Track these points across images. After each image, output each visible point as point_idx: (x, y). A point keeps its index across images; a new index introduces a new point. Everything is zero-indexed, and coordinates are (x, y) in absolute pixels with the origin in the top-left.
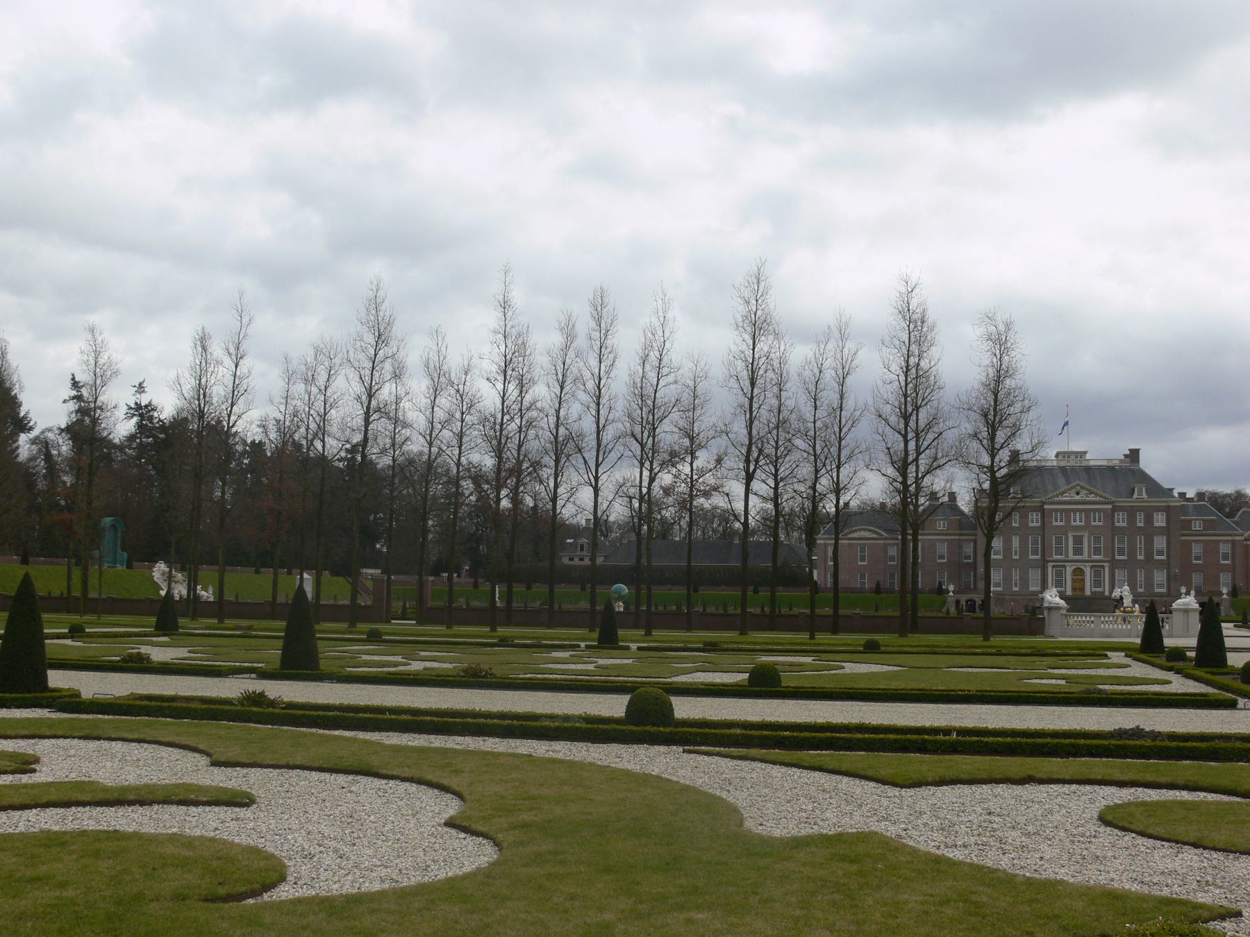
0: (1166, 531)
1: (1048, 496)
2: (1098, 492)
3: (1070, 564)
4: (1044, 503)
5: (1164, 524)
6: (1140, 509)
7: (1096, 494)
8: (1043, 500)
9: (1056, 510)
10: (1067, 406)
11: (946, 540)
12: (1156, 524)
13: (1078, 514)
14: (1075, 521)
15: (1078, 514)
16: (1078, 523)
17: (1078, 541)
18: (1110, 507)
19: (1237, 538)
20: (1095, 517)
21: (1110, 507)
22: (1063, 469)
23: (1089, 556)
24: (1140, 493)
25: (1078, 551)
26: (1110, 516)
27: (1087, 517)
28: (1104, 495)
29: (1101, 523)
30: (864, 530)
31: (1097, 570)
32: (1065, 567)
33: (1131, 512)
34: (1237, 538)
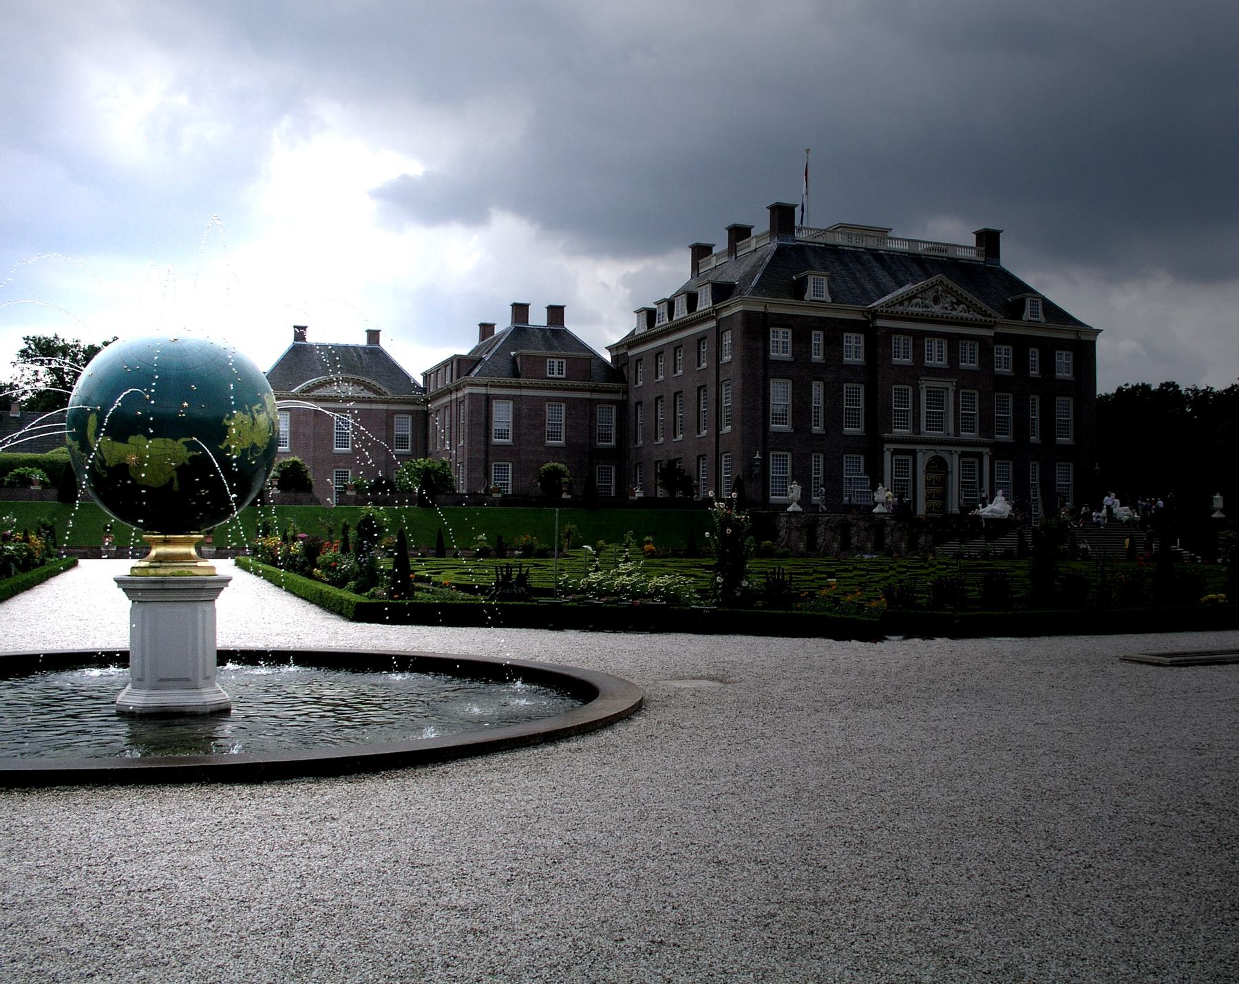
3: (923, 447)
4: (875, 315)
7: (970, 306)
10: (808, 151)
11: (564, 400)
17: (936, 398)
23: (957, 433)
25: (936, 421)
29: (975, 366)
31: (970, 458)
32: (913, 453)
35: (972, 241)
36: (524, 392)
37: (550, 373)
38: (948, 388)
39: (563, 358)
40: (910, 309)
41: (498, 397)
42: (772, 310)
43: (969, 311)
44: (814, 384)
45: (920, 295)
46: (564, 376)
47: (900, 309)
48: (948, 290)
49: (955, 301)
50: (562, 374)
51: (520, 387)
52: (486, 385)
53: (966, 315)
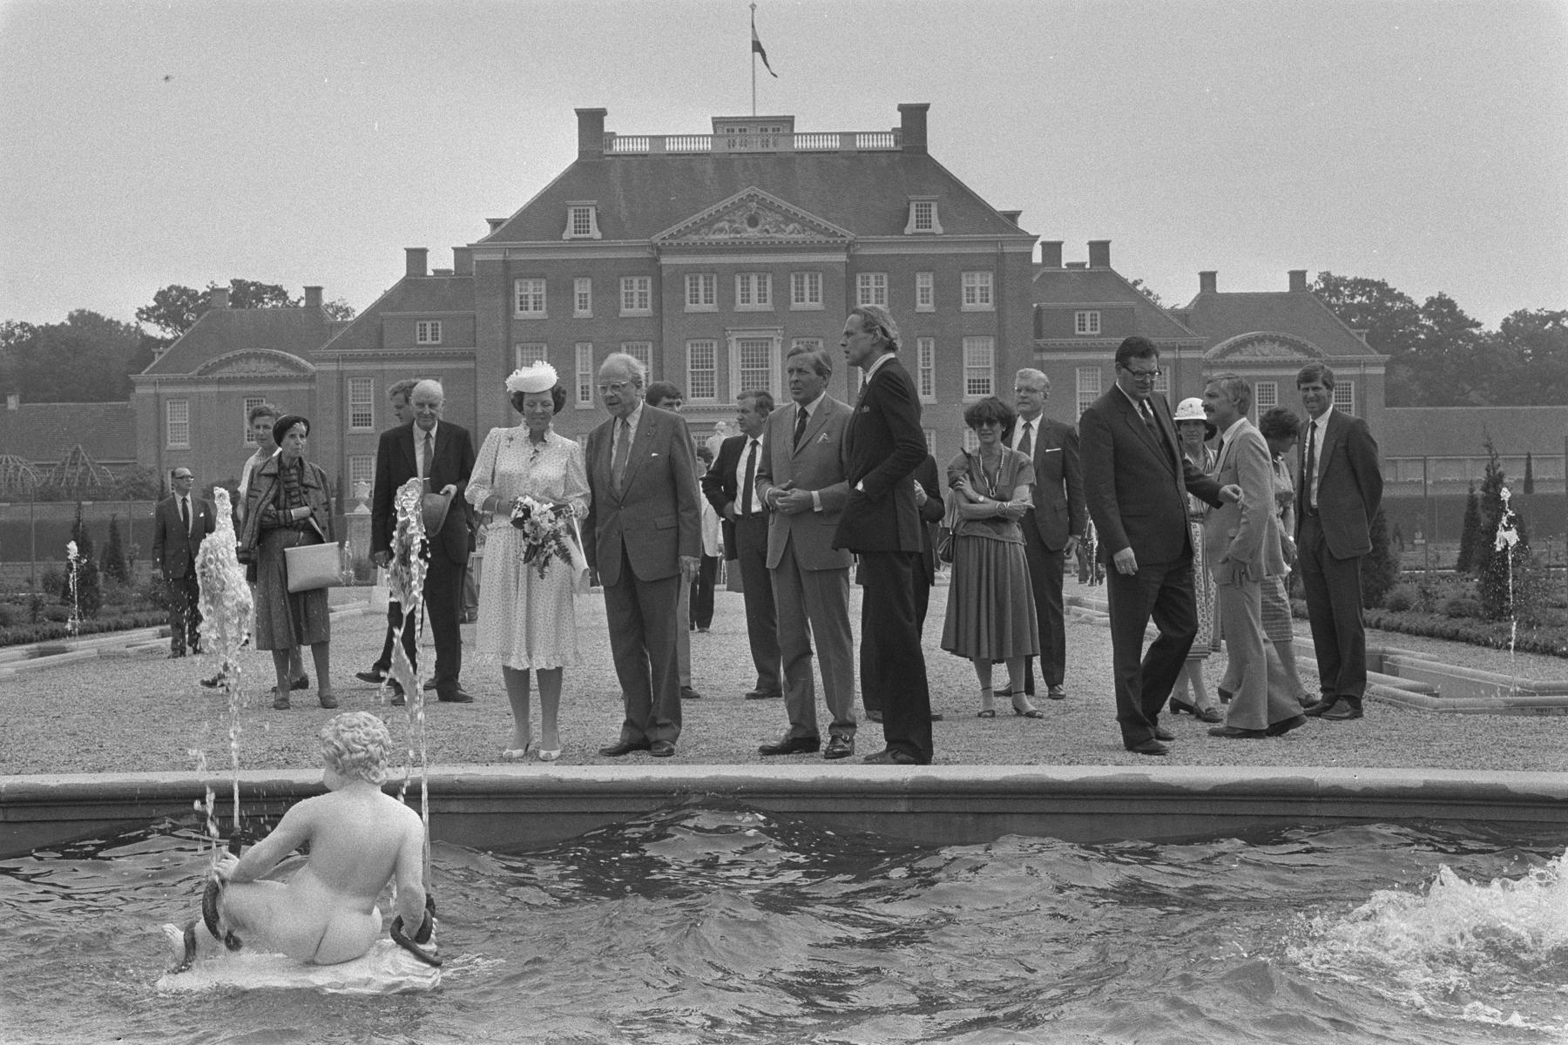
0: (996, 327)
1: (674, 229)
2: (809, 216)
4: (660, 250)
5: (988, 307)
6: (927, 264)
7: (806, 225)
8: (656, 239)
9: (695, 270)
10: (753, 7)
12: (967, 306)
13: (754, 280)
14: (746, 299)
15: (754, 280)
16: (755, 305)
18: (842, 257)
19: (1185, 355)
20: (800, 289)
21: (842, 257)
22: (722, 162)
24: (924, 221)
26: (845, 283)
27: (781, 290)
28: (824, 223)
29: (818, 305)
30: (257, 356)
33: (901, 274)
34: (1185, 355)
35: (896, 121)
36: (387, 366)
37: (421, 339)
38: (772, 339)
39: (438, 319)
40: (713, 237)
41: (353, 375)
42: (515, 257)
43: (804, 231)
44: (578, 349)
45: (727, 218)
46: (439, 342)
47: (695, 238)
48: (771, 207)
49: (781, 219)
50: (437, 339)
51: (382, 359)
52: (338, 360)
53: (802, 235)
